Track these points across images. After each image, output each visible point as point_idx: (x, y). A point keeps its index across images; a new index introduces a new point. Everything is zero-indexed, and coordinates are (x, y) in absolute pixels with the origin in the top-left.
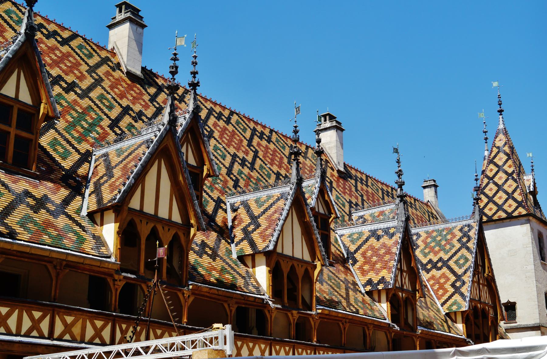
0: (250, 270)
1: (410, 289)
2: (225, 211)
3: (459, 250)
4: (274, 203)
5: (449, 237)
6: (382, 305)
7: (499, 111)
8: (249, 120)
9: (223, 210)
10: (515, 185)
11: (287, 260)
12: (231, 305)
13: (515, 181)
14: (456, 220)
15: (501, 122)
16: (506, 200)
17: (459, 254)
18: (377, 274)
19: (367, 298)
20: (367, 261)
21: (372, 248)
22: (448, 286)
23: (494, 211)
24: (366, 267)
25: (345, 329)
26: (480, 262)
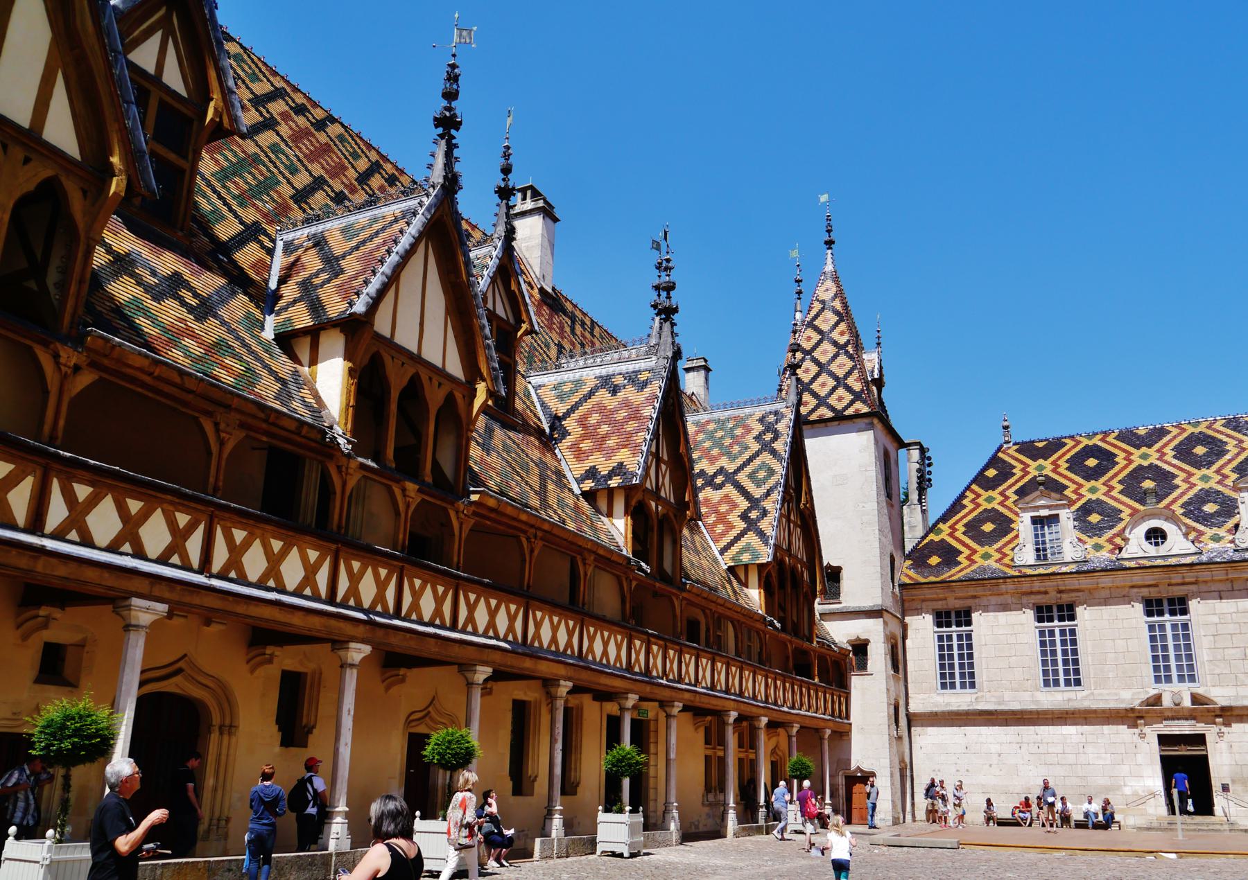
0: (305, 370)
1: (672, 500)
2: (270, 252)
3: (757, 454)
4: (384, 228)
5: (738, 432)
6: (615, 521)
7: (826, 243)
8: (369, 146)
9: (263, 247)
10: (850, 364)
11: (404, 359)
12: (222, 426)
13: (851, 357)
14: (752, 403)
15: (829, 261)
16: (834, 389)
17: (757, 462)
18: (609, 458)
19: (583, 503)
20: (589, 432)
21: (601, 408)
22: (734, 518)
23: (810, 407)
24: (586, 445)
25: (532, 551)
26: (792, 482)
